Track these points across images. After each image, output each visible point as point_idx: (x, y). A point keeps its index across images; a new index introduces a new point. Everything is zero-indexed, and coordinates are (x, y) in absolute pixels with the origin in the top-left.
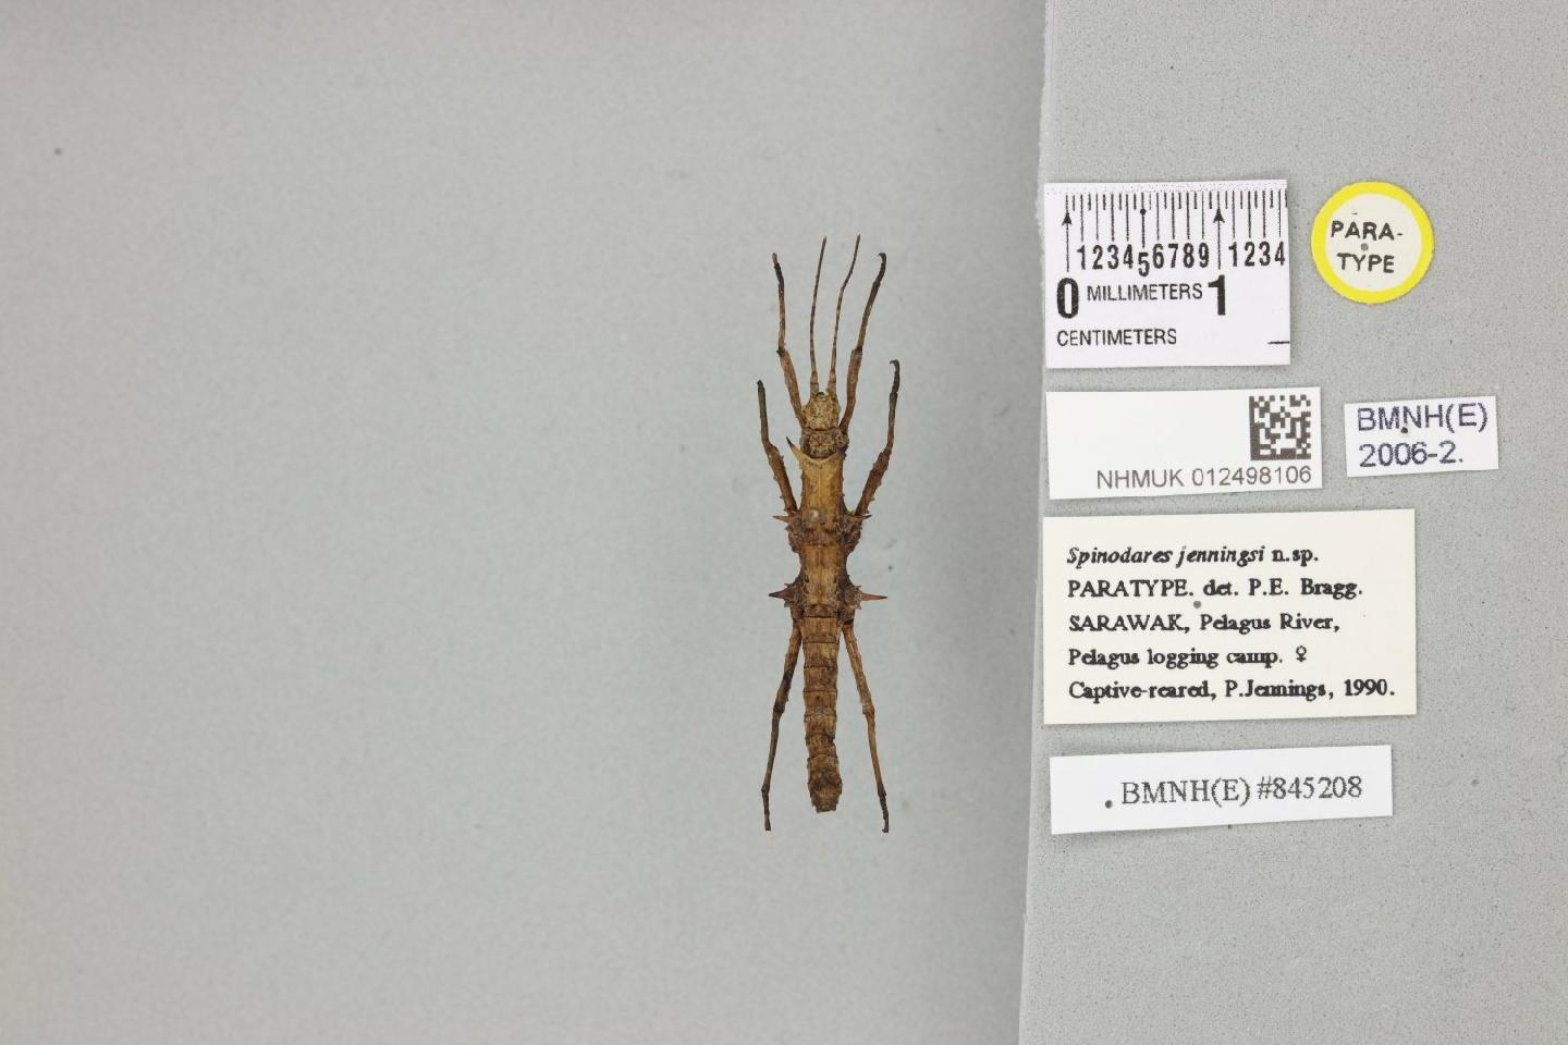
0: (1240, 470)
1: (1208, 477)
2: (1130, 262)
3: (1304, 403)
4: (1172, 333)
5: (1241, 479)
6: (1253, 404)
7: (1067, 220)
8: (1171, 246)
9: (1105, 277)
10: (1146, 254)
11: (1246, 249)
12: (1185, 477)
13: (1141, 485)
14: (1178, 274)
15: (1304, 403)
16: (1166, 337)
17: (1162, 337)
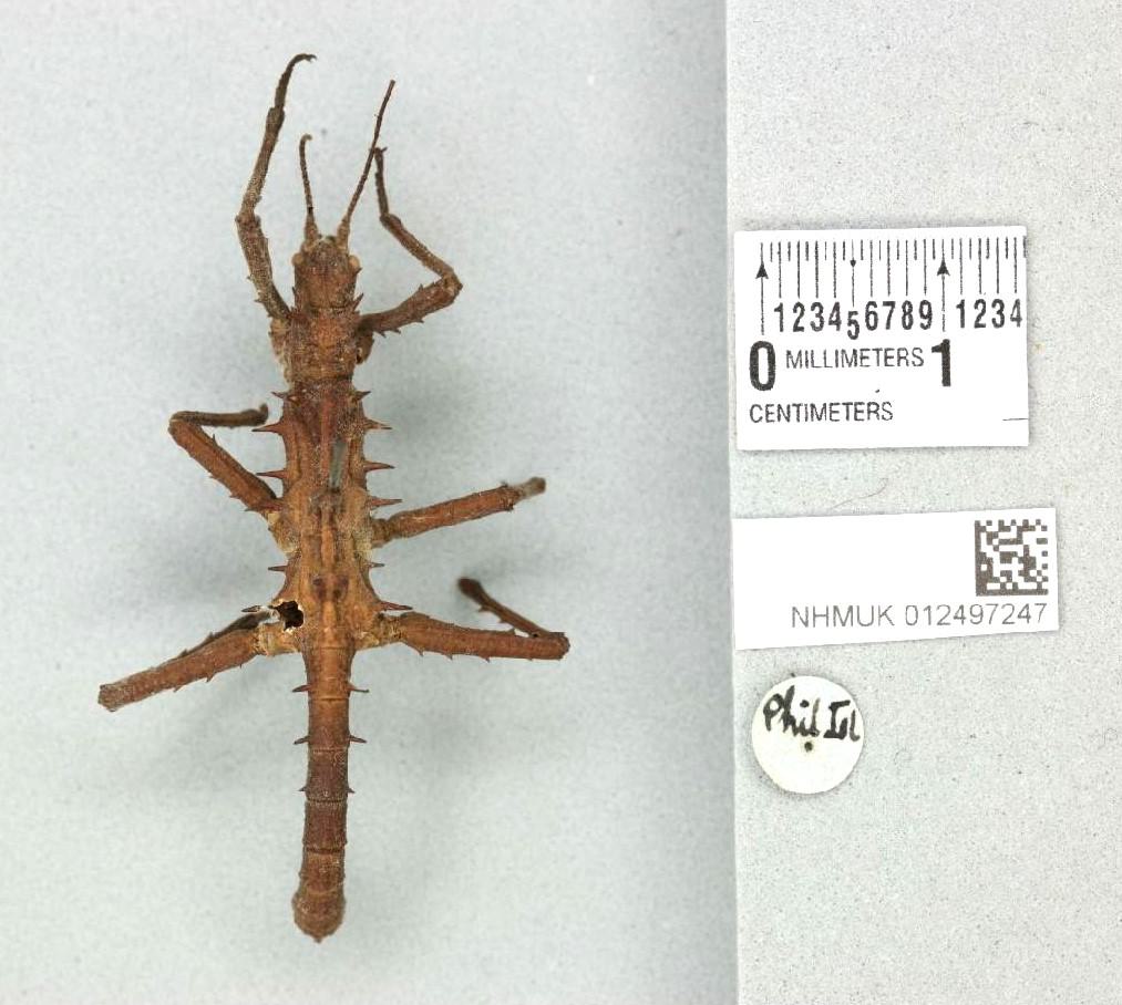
0: (962, 607)
1: (923, 615)
2: (837, 323)
3: (1038, 528)
4: (887, 407)
5: (963, 618)
6: (979, 528)
7: (762, 273)
8: (886, 304)
9: (807, 341)
10: (856, 313)
11: (976, 307)
12: (897, 614)
13: (844, 624)
14: (895, 337)
15: (1038, 528)
16: (881, 412)
17: (875, 412)
